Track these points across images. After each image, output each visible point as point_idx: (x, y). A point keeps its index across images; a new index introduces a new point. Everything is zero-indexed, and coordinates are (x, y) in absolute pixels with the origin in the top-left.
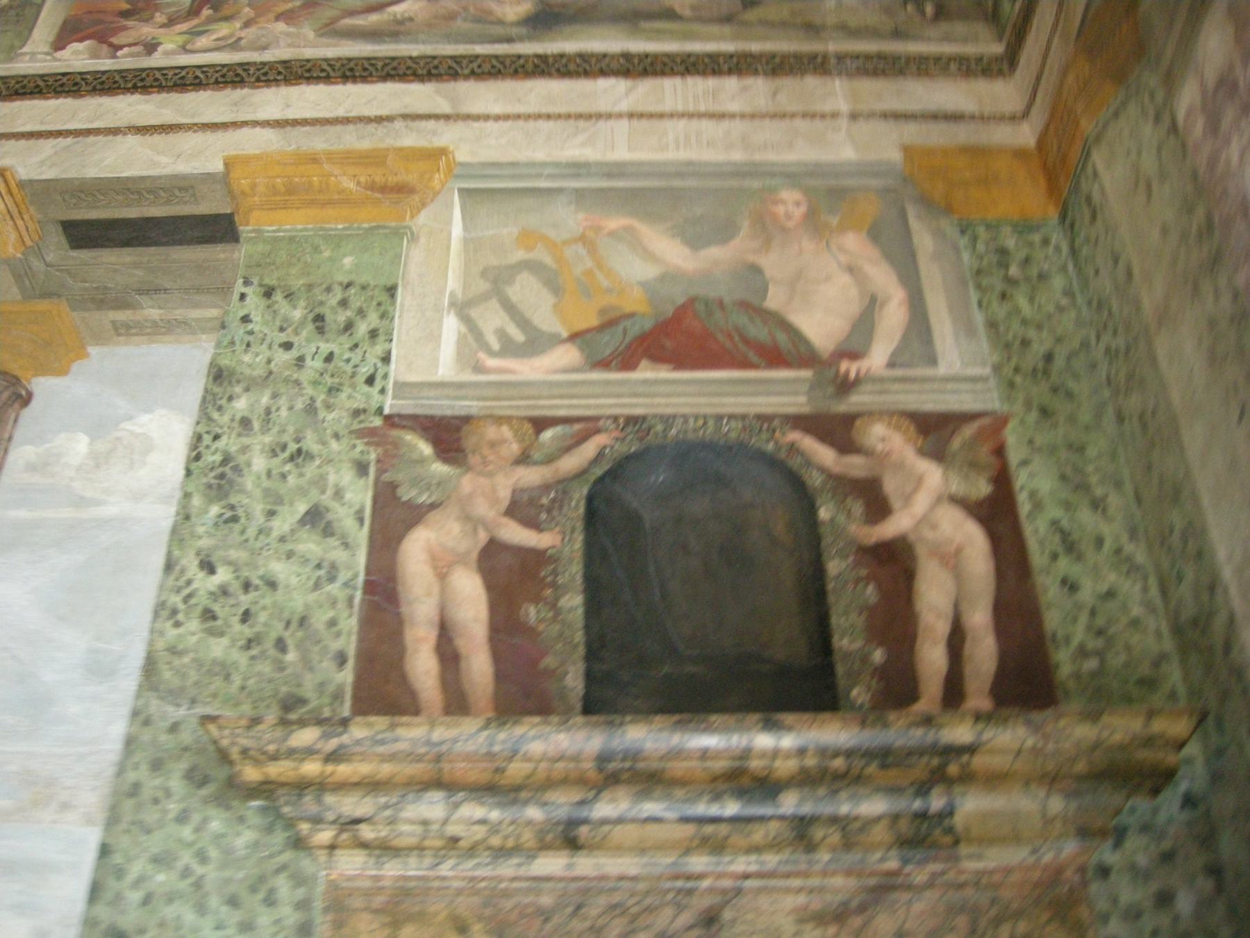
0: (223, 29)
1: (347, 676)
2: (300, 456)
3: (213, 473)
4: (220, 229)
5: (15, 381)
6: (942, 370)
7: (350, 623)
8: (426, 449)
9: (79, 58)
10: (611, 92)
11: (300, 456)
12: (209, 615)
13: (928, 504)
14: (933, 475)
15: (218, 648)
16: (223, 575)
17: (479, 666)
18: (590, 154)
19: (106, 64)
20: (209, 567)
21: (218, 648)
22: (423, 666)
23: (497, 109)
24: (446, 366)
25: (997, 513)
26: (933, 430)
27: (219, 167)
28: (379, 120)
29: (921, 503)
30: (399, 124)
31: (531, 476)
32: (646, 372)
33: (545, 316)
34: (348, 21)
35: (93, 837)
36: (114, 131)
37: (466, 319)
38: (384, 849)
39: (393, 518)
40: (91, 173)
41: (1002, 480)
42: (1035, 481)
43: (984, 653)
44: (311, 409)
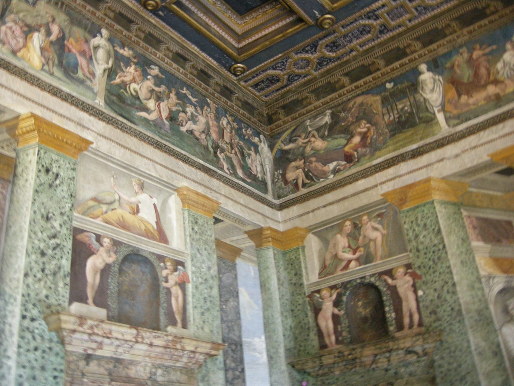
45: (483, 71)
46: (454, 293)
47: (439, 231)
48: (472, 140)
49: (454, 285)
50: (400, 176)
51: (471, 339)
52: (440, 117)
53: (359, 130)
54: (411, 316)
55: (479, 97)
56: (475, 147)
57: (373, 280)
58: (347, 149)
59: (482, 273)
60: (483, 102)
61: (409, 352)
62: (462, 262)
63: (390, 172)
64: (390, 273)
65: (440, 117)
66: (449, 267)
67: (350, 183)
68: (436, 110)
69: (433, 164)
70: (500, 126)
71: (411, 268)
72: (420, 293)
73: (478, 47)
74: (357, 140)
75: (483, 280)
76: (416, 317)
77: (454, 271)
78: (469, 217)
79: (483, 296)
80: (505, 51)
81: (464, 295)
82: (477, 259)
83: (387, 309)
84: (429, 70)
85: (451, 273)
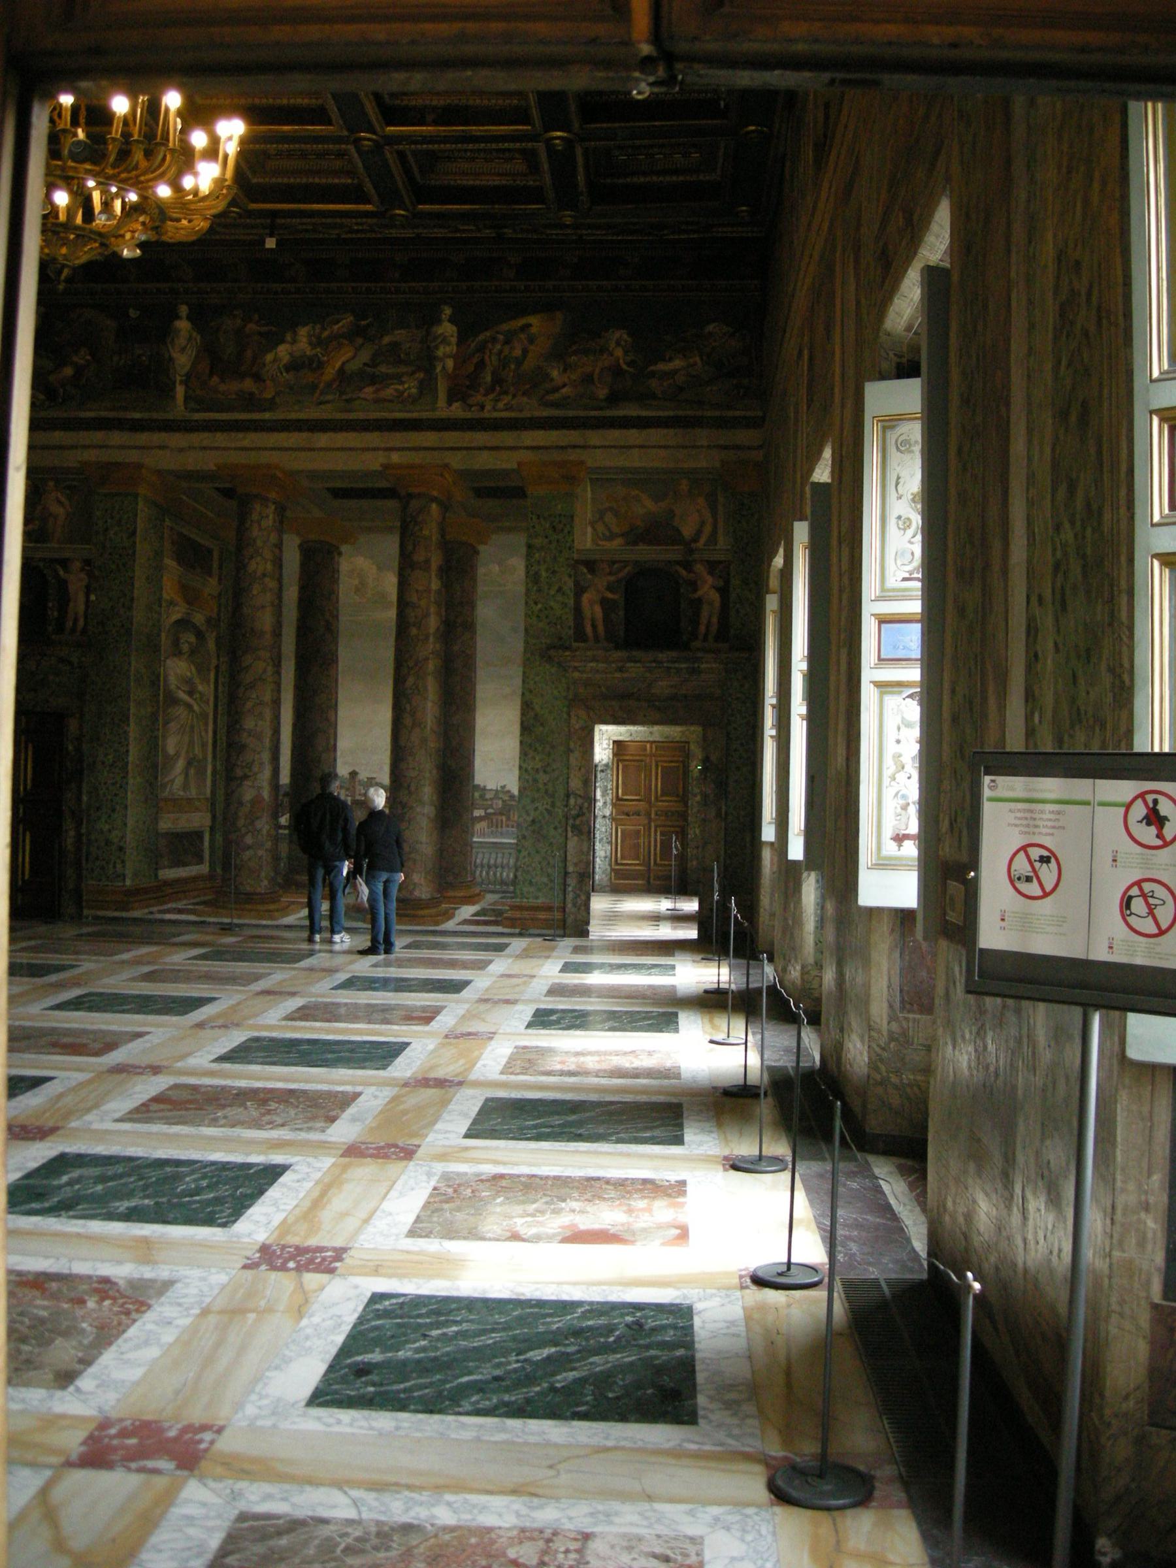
0: (506, 399)
1: (571, 632)
2: (554, 572)
3: (533, 578)
4: (519, 493)
5: (473, 547)
6: (718, 547)
7: (571, 618)
8: (585, 570)
9: (457, 411)
10: (633, 436)
11: (554, 572)
12: (538, 616)
13: (708, 590)
14: (710, 580)
15: (541, 625)
16: (540, 606)
17: (601, 629)
18: (627, 464)
19: (469, 415)
20: (536, 603)
21: (541, 625)
22: (589, 630)
23: (598, 444)
24: (589, 545)
25: (724, 591)
26: (712, 566)
27: (515, 466)
28: (562, 448)
29: (706, 588)
30: (570, 450)
31: (612, 578)
32: (641, 547)
33: (616, 530)
34: (547, 397)
35: (521, 669)
36: (480, 449)
37: (593, 527)
38: (582, 672)
39: (579, 590)
40: (477, 467)
41: (727, 582)
42: (735, 582)
43: (714, 628)
44: (555, 558)
45: (249, 354)
46: (130, 608)
47: (134, 533)
48: (204, 438)
49: (132, 599)
50: (106, 447)
51: (133, 663)
52: (180, 391)
53: (75, 359)
54: (76, 620)
55: (233, 387)
56: (205, 448)
57: (41, 564)
58: (51, 378)
59: (165, 596)
60: (234, 396)
61: (62, 660)
62: (147, 578)
63: (98, 436)
64: (64, 563)
65: (180, 391)
66: (132, 578)
67: (45, 430)
68: (178, 378)
69: (152, 448)
70: (241, 435)
71: (89, 565)
72: (93, 597)
73: (256, 317)
74: (68, 371)
75: (164, 604)
76: (81, 623)
77: (136, 586)
78: (172, 529)
79: (159, 621)
80: (283, 341)
81: (139, 616)
82: (165, 578)
83: (50, 605)
84: (189, 318)
85: (133, 585)
